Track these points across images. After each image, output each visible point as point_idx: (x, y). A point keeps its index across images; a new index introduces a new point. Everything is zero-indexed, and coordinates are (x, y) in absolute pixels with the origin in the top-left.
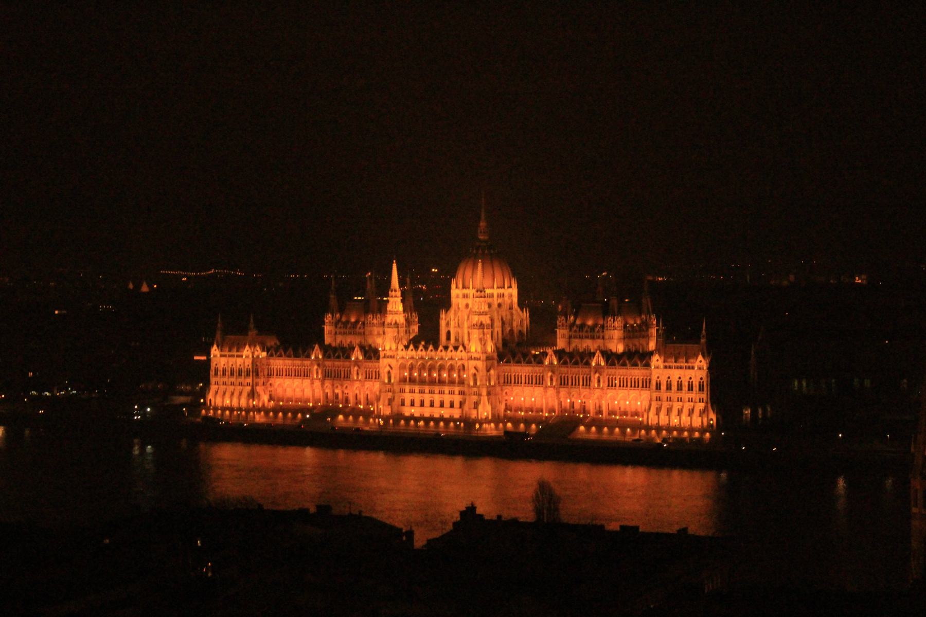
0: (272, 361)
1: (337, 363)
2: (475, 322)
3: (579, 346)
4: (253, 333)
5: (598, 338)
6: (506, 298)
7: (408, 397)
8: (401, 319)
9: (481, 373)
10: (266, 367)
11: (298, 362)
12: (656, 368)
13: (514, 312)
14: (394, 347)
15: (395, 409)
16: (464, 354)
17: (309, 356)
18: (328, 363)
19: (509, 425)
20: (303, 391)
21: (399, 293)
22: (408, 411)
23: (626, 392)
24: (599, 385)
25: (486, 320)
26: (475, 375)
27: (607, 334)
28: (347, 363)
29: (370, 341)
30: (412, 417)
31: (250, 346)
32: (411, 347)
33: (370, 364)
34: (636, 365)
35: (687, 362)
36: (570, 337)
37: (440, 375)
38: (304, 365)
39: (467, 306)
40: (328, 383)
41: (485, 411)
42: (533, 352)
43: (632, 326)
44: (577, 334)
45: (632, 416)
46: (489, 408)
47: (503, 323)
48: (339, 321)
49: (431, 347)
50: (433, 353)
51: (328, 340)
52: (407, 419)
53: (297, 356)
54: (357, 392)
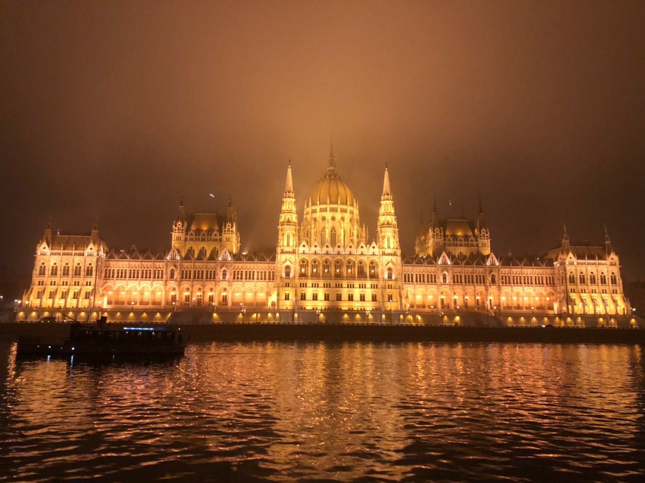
1: (196, 264)
5: (472, 245)
7: (309, 292)
8: (294, 218)
16: (377, 251)
18: (187, 265)
19: (419, 318)
22: (309, 305)
24: (493, 281)
26: (390, 269)
27: (480, 241)
31: (94, 243)
33: (240, 265)
36: (445, 245)
39: (333, 219)
40: (186, 284)
51: (175, 244)
53: (148, 258)
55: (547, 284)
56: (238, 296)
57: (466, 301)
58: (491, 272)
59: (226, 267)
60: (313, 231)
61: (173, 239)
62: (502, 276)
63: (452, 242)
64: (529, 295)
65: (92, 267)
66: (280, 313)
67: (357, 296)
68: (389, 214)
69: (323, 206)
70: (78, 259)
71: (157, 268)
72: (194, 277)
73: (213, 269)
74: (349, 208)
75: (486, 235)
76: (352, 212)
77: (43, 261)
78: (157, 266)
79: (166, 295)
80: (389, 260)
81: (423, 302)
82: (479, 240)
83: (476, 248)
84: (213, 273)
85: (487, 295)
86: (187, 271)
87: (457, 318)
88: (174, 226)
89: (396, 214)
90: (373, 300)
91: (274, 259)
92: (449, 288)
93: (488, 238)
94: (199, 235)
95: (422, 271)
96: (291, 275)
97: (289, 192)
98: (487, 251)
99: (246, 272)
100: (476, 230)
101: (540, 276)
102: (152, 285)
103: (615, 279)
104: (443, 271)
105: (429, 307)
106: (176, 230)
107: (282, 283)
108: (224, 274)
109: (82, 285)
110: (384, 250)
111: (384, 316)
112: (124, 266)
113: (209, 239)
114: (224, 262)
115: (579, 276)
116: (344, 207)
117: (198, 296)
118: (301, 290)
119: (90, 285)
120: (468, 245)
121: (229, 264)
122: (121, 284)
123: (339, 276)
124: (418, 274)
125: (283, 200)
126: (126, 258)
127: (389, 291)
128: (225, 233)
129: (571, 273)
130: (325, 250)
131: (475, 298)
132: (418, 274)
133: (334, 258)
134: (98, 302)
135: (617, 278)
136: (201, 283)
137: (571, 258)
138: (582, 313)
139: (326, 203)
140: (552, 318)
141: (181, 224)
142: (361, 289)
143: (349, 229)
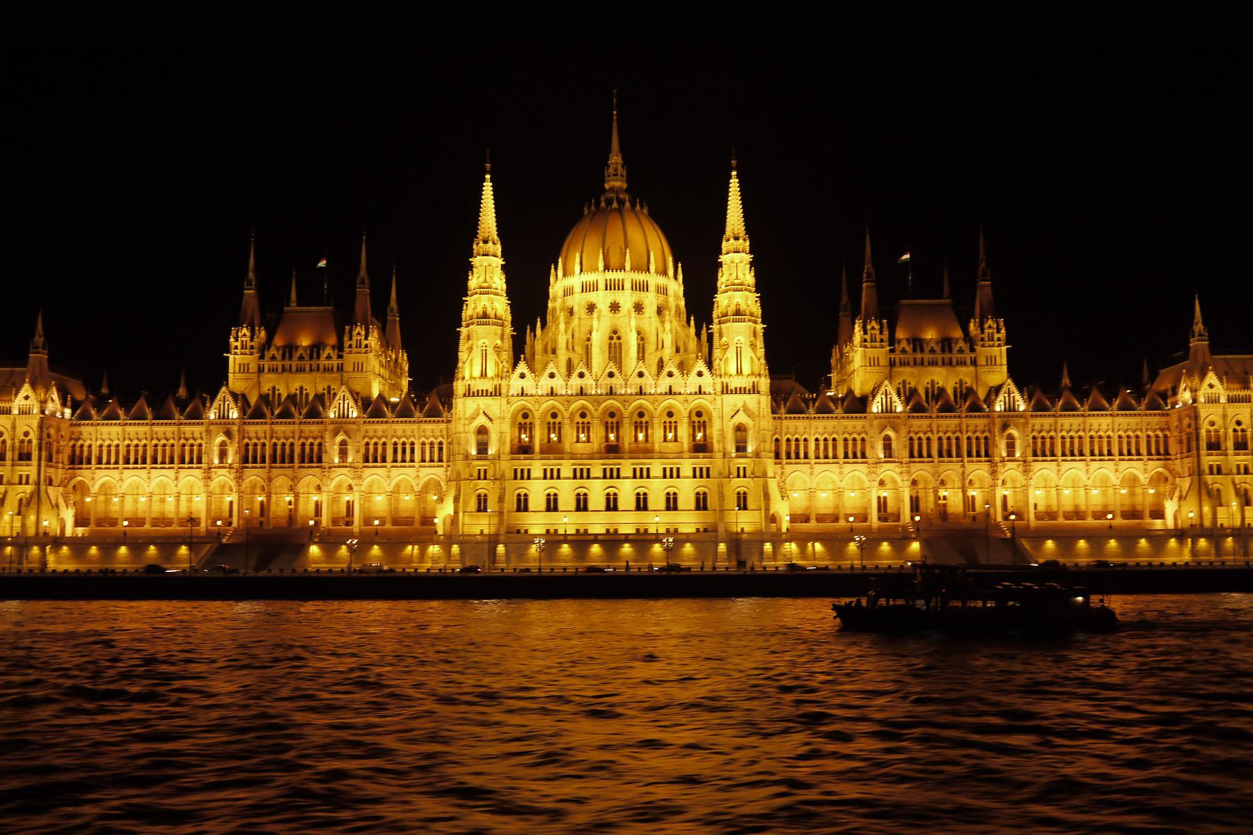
1: (277, 428)
4: (38, 357)
5: (962, 363)
7: (537, 491)
8: (501, 306)
10: (66, 446)
11: (165, 430)
16: (707, 381)
17: (196, 415)
18: (256, 430)
22: (536, 523)
24: (1011, 452)
26: (740, 429)
27: (983, 352)
28: (312, 428)
29: (357, 387)
31: (34, 386)
33: (380, 427)
34: (1097, 408)
36: (892, 364)
39: (615, 307)
40: (254, 476)
51: (235, 381)
53: (161, 414)
55: (1149, 453)
56: (380, 503)
57: (942, 502)
58: (1005, 427)
59: (346, 433)
60: (562, 340)
61: (231, 370)
62: (1034, 438)
63: (909, 357)
64: (1104, 484)
65: (30, 442)
66: (460, 543)
67: (657, 501)
68: (739, 287)
69: (589, 277)
71: (187, 439)
72: (274, 460)
73: (315, 438)
74: (654, 279)
75: (996, 336)
76: (662, 291)
78: (188, 435)
79: (209, 503)
80: (740, 404)
81: (837, 507)
82: (978, 348)
83: (972, 369)
84: (316, 448)
85: (994, 486)
86: (256, 445)
87: (915, 546)
88: (232, 340)
89: (759, 287)
90: (698, 508)
91: (450, 407)
92: (898, 470)
93: (1002, 343)
94: (291, 358)
95: (830, 430)
96: (492, 451)
97: (486, 242)
98: (999, 375)
99: (395, 444)
100: (972, 325)
101: (1130, 433)
102: (177, 479)
104: (883, 428)
105: (847, 517)
106: (236, 348)
107: (468, 470)
108: (343, 453)
109: (9, 483)
110: (726, 380)
111: (722, 547)
112: (113, 436)
113: (314, 367)
114: (342, 423)
115: (1230, 431)
116: (641, 277)
117: (290, 503)
118: (514, 488)
119: (27, 483)
120: (950, 364)
121: (354, 427)
122: (107, 478)
123: (613, 450)
124: (821, 438)
126: (118, 418)
127: (738, 484)
128: (350, 353)
129: (1212, 424)
130: (575, 382)
131: (964, 492)
132: (821, 438)
133: (599, 403)
134: (49, 523)
136: (289, 472)
137: (1211, 386)
138: (1238, 523)
139: (596, 269)
140: (1158, 539)
141: (248, 334)
142: (668, 480)
143: (654, 332)
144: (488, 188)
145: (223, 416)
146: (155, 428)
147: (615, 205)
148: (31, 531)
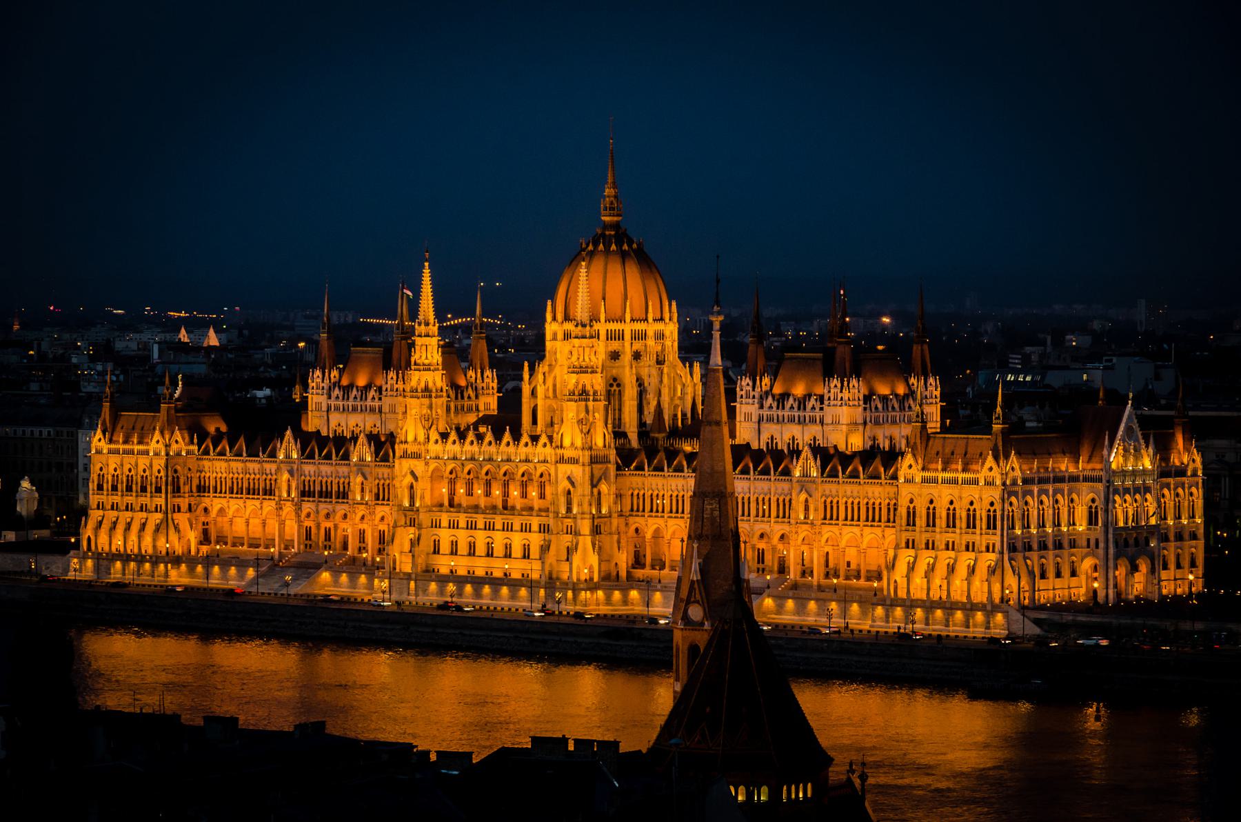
0: (207, 464)
2: (571, 386)
3: (777, 436)
5: (813, 421)
6: (651, 342)
7: (445, 536)
8: (436, 379)
9: (579, 490)
10: (195, 475)
11: (253, 466)
12: (907, 481)
13: (665, 371)
14: (421, 438)
15: (421, 561)
16: (548, 450)
17: (273, 455)
18: (309, 468)
20: (264, 524)
21: (434, 329)
22: (444, 564)
23: (856, 529)
25: (597, 382)
27: (829, 413)
28: (343, 470)
30: (453, 577)
32: (453, 436)
34: (876, 476)
35: (964, 470)
37: (506, 494)
38: (263, 472)
40: (308, 507)
41: (586, 564)
42: (688, 449)
43: (884, 399)
44: (774, 412)
45: (868, 579)
46: (594, 560)
47: (642, 394)
48: (337, 384)
49: (489, 437)
50: (493, 449)
52: (443, 580)
53: (253, 453)
54: (362, 526)
70: (143, 462)
77: (100, 465)
97: (420, 324)
103: (995, 516)
108: (362, 490)
114: (361, 466)
125: (417, 339)
135: (999, 517)
144: (427, 273)
145: (288, 456)
146: (249, 465)
147: (591, 247)
148: (164, 552)
